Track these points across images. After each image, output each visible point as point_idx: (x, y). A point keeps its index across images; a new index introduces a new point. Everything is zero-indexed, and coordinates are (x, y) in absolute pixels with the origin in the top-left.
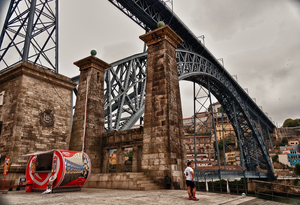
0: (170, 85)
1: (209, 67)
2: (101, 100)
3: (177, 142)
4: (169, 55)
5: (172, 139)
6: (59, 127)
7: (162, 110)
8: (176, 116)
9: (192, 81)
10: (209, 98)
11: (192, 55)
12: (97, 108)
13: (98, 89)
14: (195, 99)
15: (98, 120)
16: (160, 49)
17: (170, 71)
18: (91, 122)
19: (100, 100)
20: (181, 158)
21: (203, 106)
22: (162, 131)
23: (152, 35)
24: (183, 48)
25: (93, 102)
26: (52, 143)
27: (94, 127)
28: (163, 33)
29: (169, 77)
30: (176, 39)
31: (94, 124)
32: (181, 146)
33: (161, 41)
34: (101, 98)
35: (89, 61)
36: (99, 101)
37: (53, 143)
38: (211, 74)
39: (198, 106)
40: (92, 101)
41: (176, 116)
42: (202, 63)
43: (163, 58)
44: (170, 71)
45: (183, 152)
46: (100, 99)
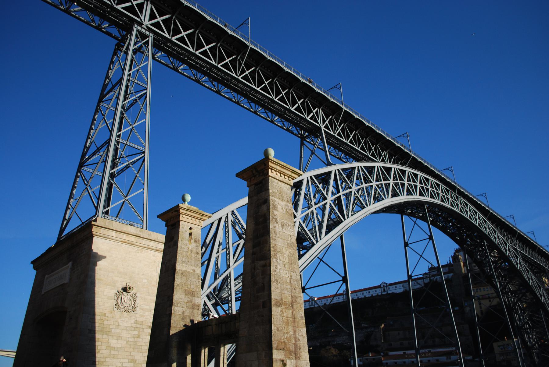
0: (275, 245)
1: (426, 185)
2: (196, 269)
3: (287, 333)
4: (275, 199)
5: (275, 328)
6: (145, 313)
7: (264, 284)
8: (286, 292)
9: (397, 212)
10: (431, 241)
11: (388, 170)
12: (189, 283)
13: (190, 252)
14: (406, 245)
15: (191, 301)
16: (263, 191)
17: (277, 223)
18: (179, 305)
19: (194, 271)
20: (296, 358)
21: (421, 256)
22: (263, 316)
23: (252, 171)
24: (368, 159)
25: (182, 273)
26: (134, 338)
27: (183, 313)
28: (265, 168)
29: (275, 232)
30: (290, 173)
31: (183, 307)
32: (295, 338)
33: (263, 179)
34: (196, 266)
35: (177, 213)
36: (192, 271)
37: (136, 339)
38: (431, 197)
39: (413, 258)
40: (180, 272)
41: (286, 292)
42: (409, 180)
43: (266, 204)
44: (277, 223)
45: (300, 349)
46: (193, 268)
